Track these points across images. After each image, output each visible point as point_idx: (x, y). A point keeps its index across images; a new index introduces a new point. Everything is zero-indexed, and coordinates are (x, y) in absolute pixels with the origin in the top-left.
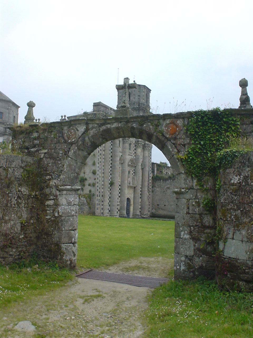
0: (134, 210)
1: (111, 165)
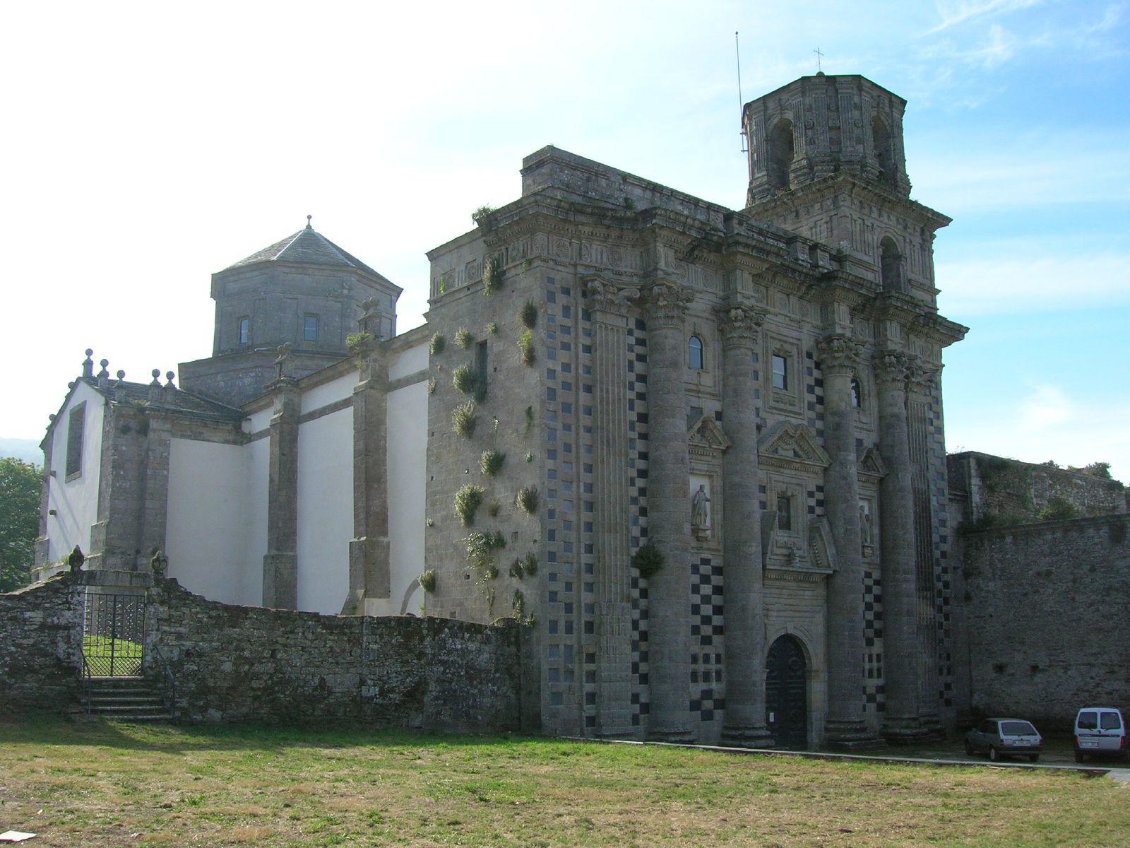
0: (831, 698)
1: (641, 464)
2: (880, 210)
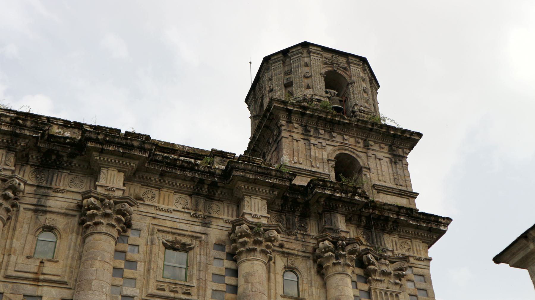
2: (330, 132)
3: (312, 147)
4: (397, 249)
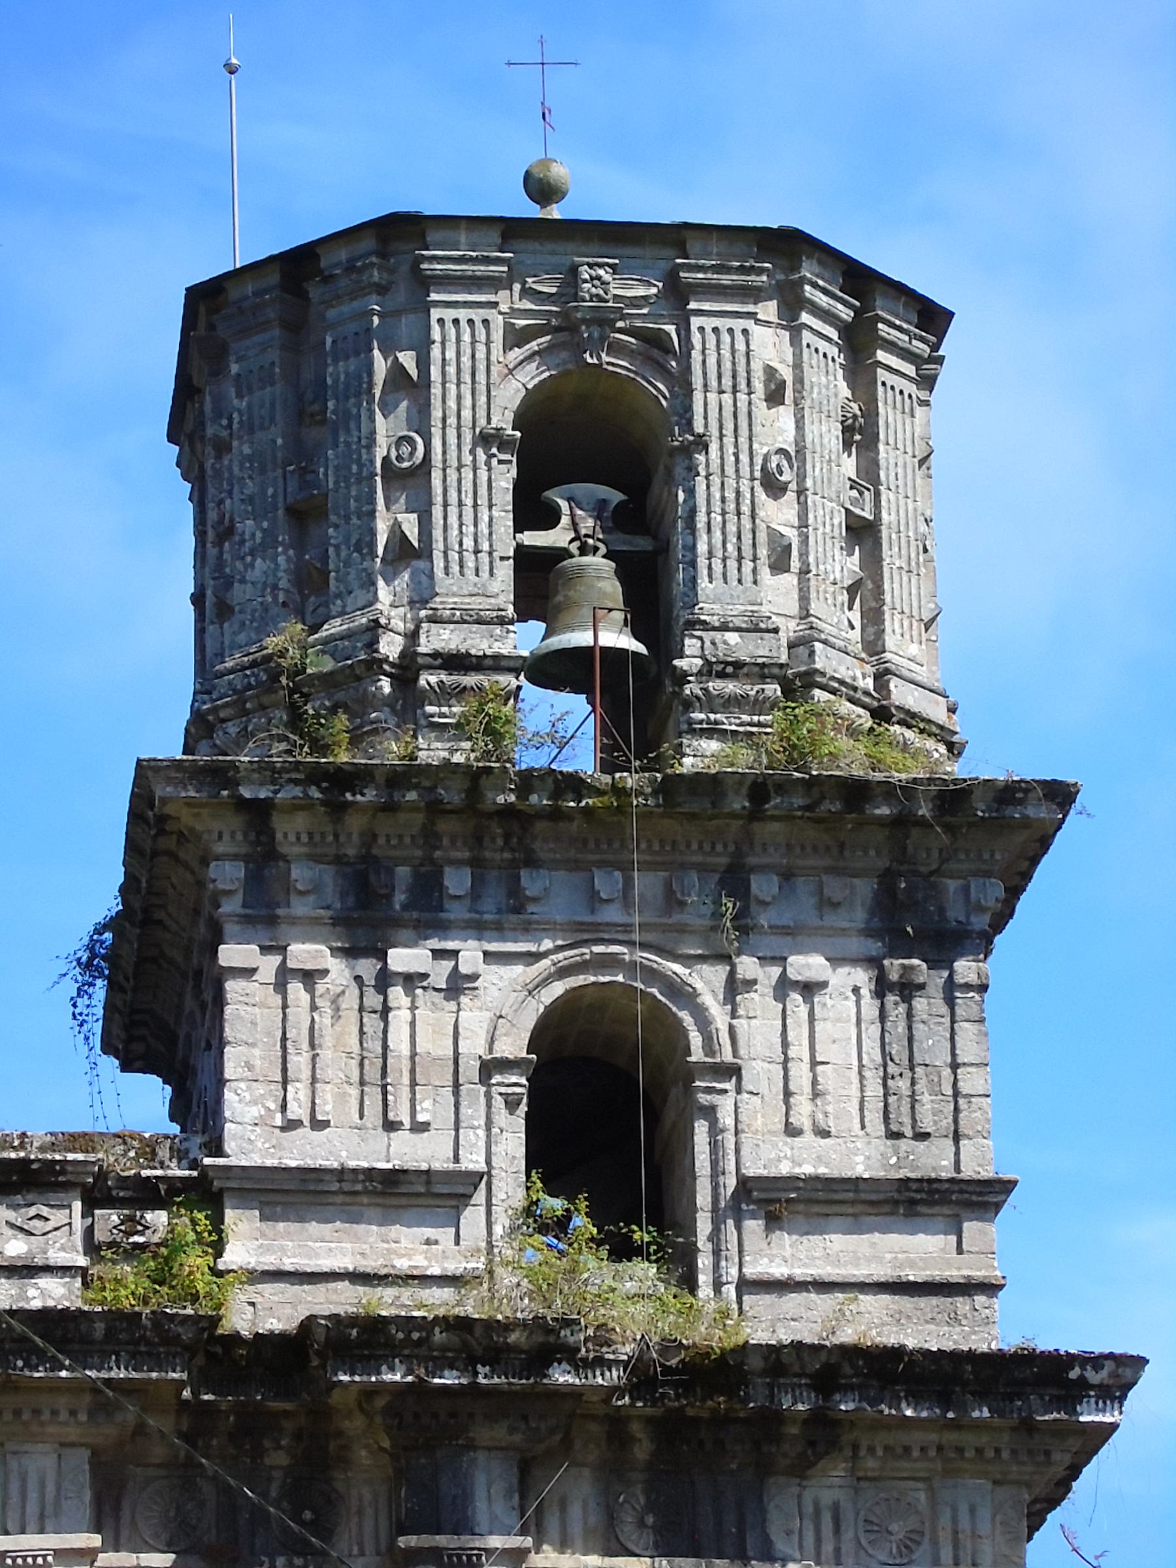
3: (397, 994)
4: (837, 1551)
